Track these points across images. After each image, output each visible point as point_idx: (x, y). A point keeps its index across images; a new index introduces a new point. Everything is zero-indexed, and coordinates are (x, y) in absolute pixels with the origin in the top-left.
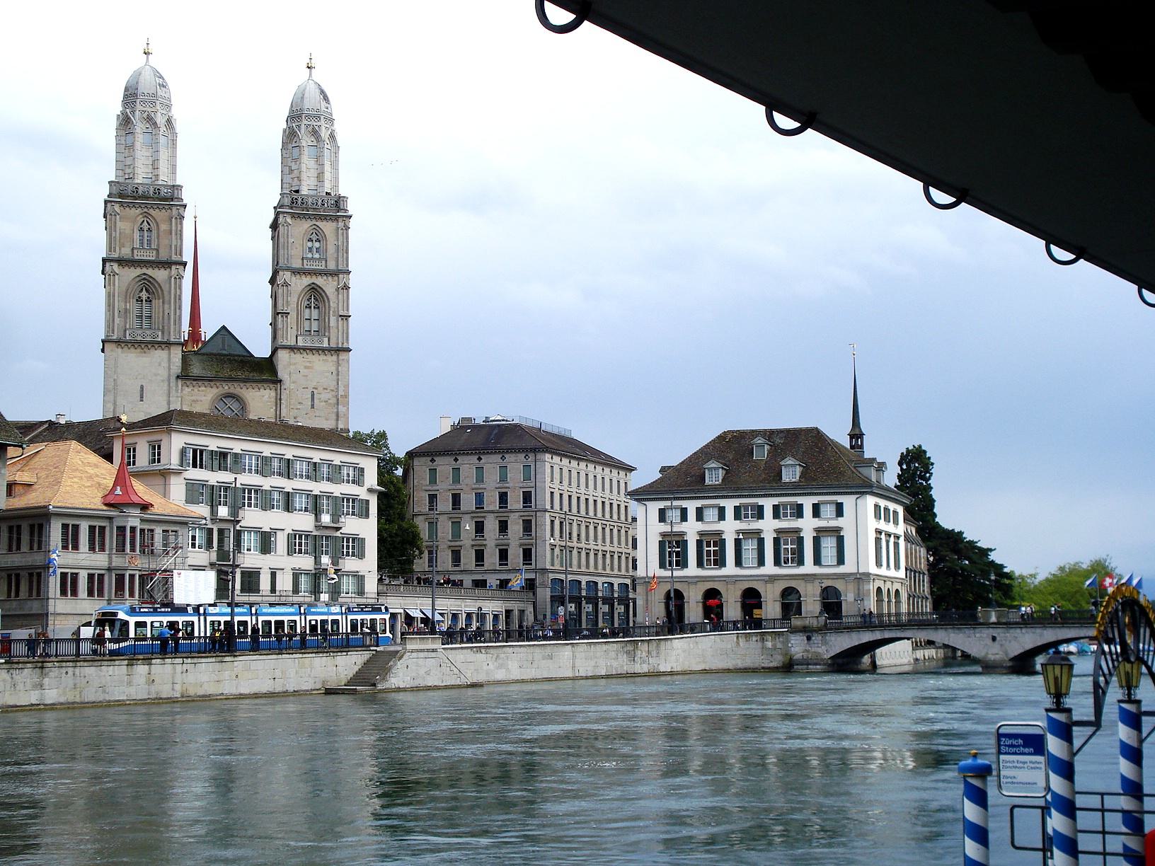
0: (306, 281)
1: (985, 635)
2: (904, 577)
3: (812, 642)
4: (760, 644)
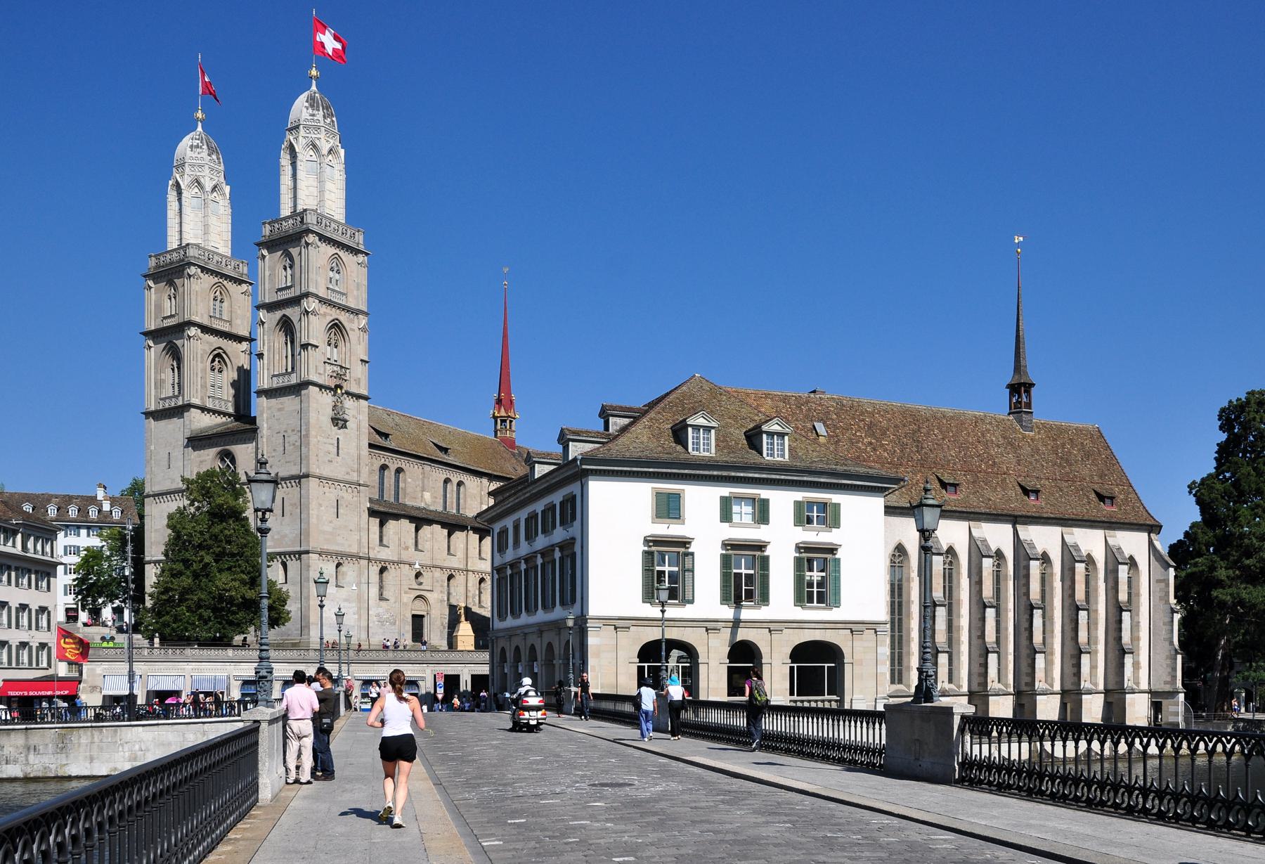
0: (278, 314)
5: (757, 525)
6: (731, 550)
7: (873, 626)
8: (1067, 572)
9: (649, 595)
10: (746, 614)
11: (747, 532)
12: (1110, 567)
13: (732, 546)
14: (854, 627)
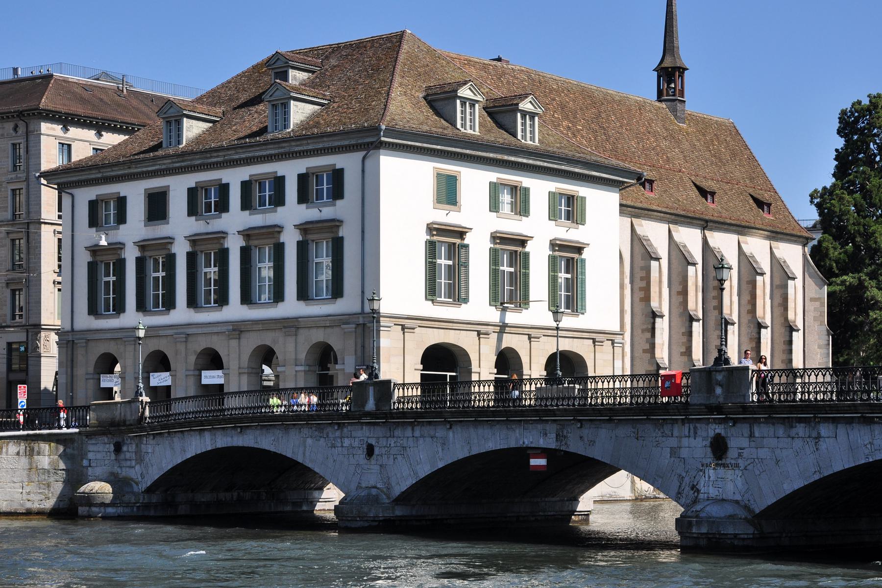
1: (356, 444)
2: (616, 328)
3: (122, 456)
4: (24, 461)
5: (518, 217)
6: (499, 244)
7: (611, 337)
8: (744, 286)
9: (432, 292)
10: (512, 318)
11: (513, 226)
12: (777, 282)
13: (498, 238)
14: (595, 337)
